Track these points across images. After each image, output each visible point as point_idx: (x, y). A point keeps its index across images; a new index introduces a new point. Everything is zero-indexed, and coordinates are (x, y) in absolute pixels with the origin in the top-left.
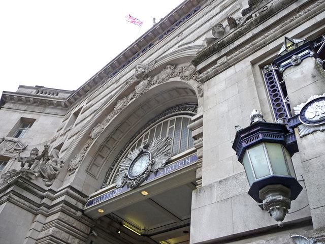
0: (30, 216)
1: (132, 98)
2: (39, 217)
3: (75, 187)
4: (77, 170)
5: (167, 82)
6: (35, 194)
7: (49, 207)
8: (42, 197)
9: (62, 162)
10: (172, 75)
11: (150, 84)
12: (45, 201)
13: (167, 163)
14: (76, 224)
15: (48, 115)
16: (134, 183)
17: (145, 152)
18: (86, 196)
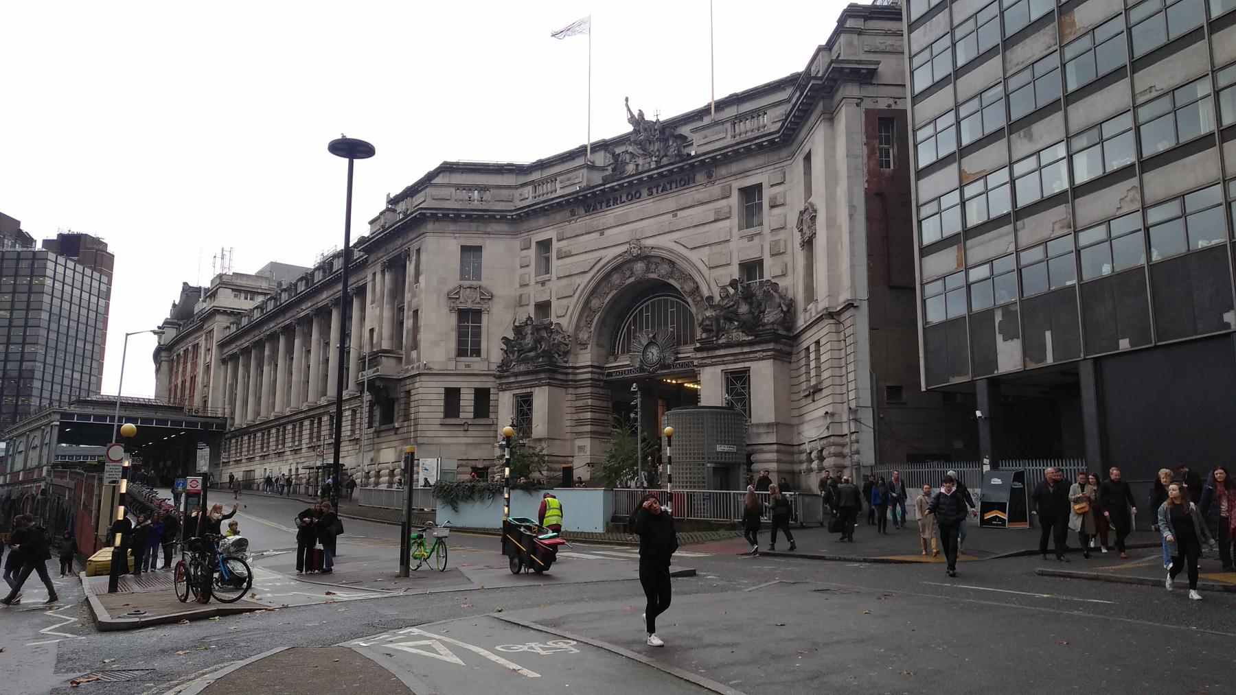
0: (564, 390)
1: (630, 277)
2: (571, 390)
3: (596, 364)
4: (589, 347)
5: (667, 281)
6: (562, 373)
7: (576, 381)
8: (567, 374)
9: (568, 336)
10: (671, 275)
11: (648, 270)
12: (571, 377)
13: (675, 360)
14: (601, 391)
15: (495, 236)
18: (602, 368)
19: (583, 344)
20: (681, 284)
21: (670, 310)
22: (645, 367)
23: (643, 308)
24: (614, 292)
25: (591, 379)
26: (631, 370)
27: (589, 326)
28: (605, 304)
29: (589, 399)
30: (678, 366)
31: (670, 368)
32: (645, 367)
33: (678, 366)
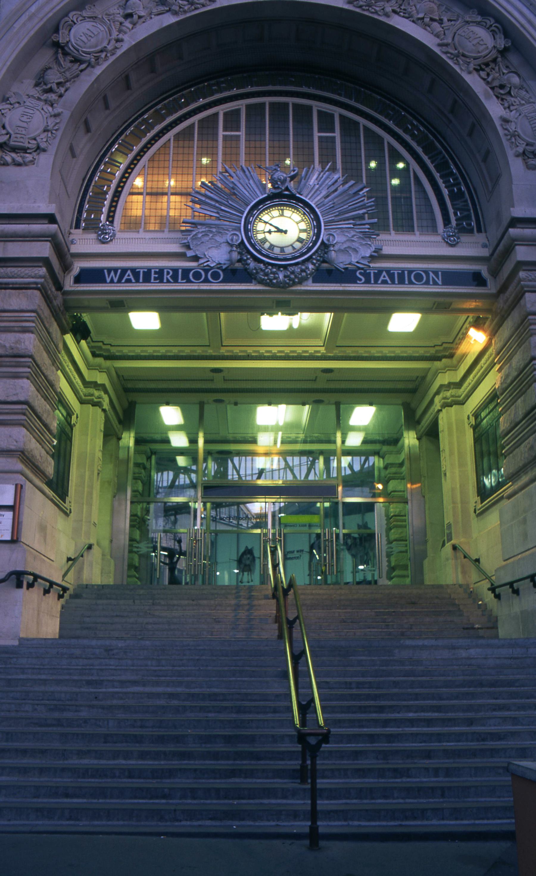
13: (372, 258)
16: (281, 276)
17: (292, 197)
19: (14, 149)
20: (437, 36)
21: (316, 134)
22: (252, 264)
23: (216, 115)
24: (170, 19)
25: (46, 262)
26: (186, 272)
27: (52, 97)
28: (125, 47)
29: (25, 330)
30: (384, 276)
31: (354, 280)
32: (252, 264)
33: (384, 276)
